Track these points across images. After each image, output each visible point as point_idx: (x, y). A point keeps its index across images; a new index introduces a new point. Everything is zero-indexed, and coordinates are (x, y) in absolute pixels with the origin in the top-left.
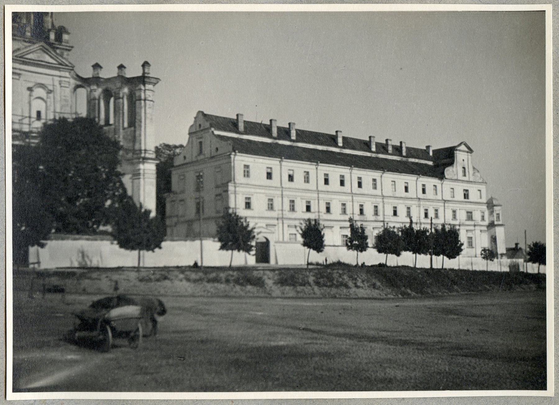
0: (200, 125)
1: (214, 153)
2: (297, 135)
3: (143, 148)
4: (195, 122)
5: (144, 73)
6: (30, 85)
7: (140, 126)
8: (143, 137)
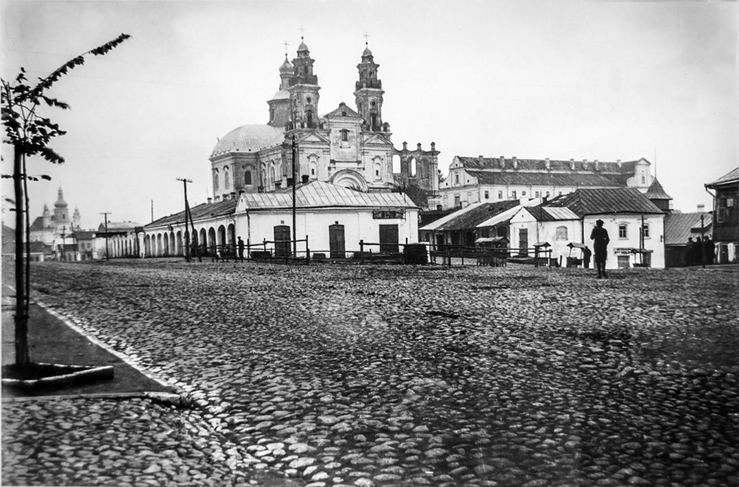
0: (457, 165)
1: (467, 184)
2: (518, 163)
5: (433, 149)
6: (373, 157)
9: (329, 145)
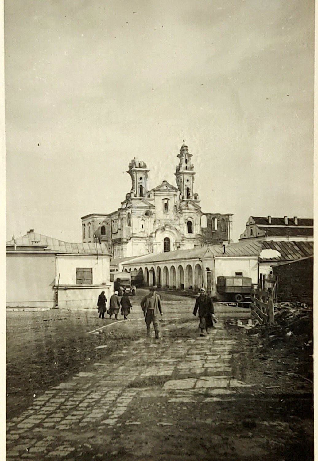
0: (251, 222)
1: (258, 235)
4: (249, 220)
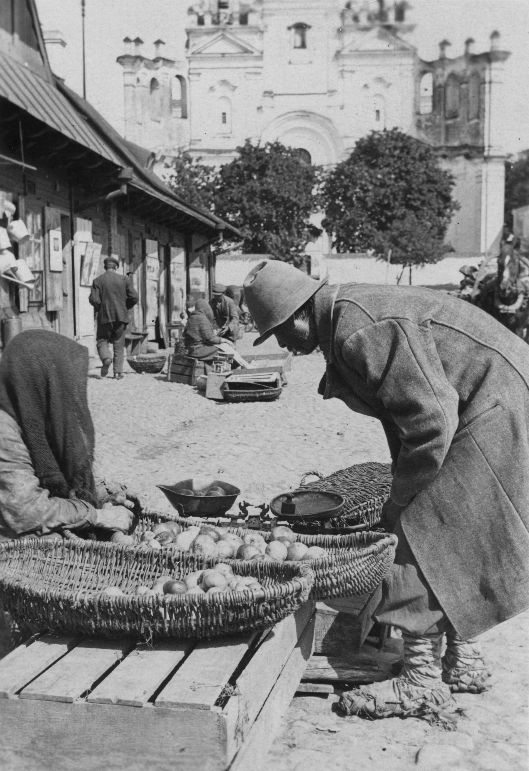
3: (486, 144)
7: (484, 117)
8: (486, 132)
9: (260, 57)
